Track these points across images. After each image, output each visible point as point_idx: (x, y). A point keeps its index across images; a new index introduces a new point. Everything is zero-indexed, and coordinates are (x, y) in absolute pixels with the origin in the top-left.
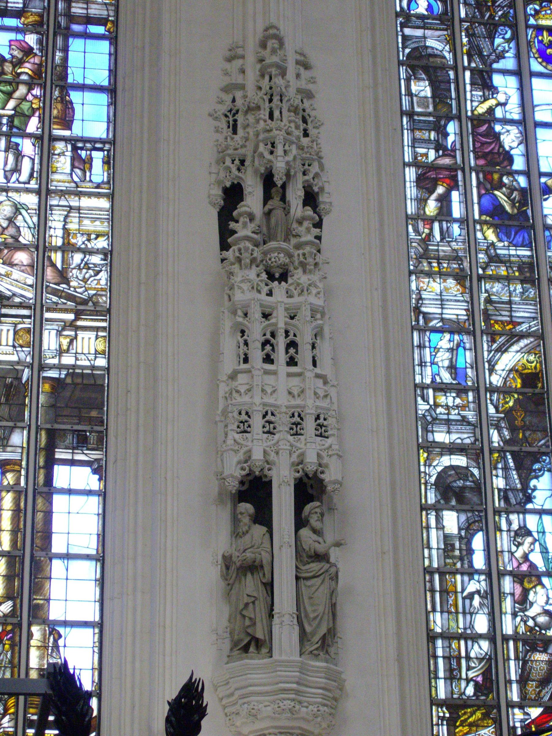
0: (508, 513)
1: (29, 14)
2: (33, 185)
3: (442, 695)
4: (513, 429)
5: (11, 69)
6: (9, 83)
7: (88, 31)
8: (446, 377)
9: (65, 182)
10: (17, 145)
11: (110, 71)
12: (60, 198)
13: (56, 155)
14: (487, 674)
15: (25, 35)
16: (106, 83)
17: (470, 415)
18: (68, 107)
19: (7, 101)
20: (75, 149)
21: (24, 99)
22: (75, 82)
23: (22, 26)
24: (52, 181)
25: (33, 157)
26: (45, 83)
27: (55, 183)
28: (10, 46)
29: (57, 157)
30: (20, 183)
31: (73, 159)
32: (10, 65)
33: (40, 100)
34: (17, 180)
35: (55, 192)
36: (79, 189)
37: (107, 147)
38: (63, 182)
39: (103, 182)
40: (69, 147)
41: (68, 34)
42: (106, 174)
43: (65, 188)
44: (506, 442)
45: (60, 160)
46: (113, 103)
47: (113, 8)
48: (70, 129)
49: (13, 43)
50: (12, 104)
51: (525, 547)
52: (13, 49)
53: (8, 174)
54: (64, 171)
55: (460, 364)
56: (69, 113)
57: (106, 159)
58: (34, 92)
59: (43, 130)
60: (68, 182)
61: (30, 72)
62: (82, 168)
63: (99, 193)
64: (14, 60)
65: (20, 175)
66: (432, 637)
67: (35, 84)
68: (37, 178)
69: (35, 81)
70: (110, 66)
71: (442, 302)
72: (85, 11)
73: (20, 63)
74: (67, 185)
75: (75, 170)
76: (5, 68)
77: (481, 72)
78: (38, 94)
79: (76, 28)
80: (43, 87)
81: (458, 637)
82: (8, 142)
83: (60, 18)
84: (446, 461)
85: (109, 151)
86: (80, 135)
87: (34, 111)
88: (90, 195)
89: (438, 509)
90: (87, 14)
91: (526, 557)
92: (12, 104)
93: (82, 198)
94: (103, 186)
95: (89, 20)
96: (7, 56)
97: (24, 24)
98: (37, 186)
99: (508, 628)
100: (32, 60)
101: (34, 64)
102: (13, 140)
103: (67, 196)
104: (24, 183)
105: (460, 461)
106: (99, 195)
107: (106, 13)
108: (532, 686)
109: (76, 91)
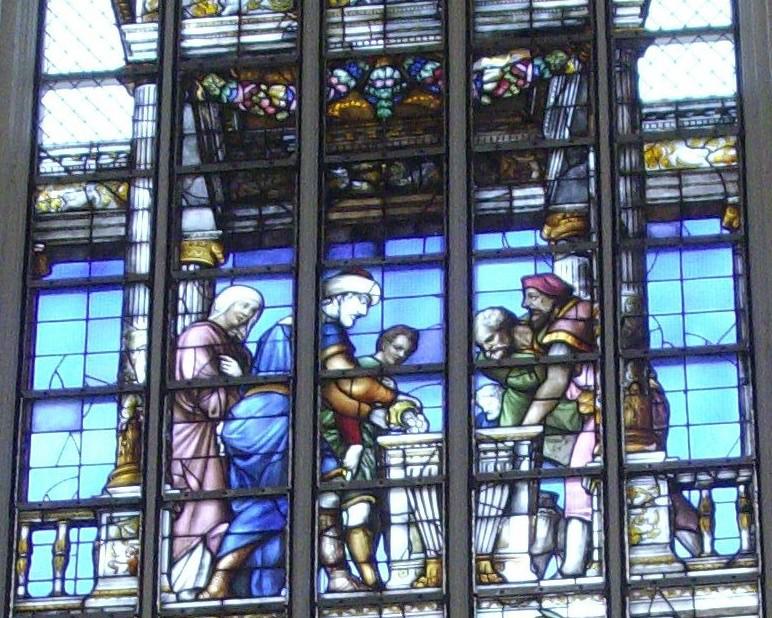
1: (559, 216)
2: (593, 578)
5: (529, 337)
6: (527, 368)
7: (685, 234)
9: (661, 562)
10: (554, 497)
11: (738, 311)
12: (652, 598)
13: (636, 507)
15: (554, 261)
16: (731, 339)
18: (655, 403)
19: (527, 408)
20: (676, 489)
21: (560, 398)
22: (666, 346)
23: (545, 243)
24: (632, 564)
25: (588, 518)
26: (603, 357)
27: (639, 568)
28: (524, 290)
29: (639, 511)
30: (565, 576)
31: (673, 512)
32: (527, 329)
33: (595, 395)
34: (560, 571)
35: (640, 586)
36: (692, 574)
37: (744, 475)
38: (654, 563)
39: (740, 553)
40: (664, 488)
41: (644, 246)
42: (745, 534)
43: (660, 576)
45: (645, 516)
46: (749, 380)
47: (735, 177)
48: (662, 447)
49: (529, 283)
50: (535, 412)
52: (531, 296)
53: (540, 561)
54: (657, 540)
56: (658, 415)
57: (743, 502)
58: (581, 380)
59: (605, 459)
60: (667, 563)
61: (569, 339)
62: (693, 526)
63: (734, 576)
64: (535, 318)
65: (564, 560)
67: (583, 363)
68: (600, 561)
69: (582, 357)
70: (736, 302)
72: (675, 193)
73: (547, 322)
74: (664, 567)
75: (679, 534)
76: (517, 337)
78: (591, 382)
79: (659, 230)
80: (598, 366)
82: (535, 494)
83: (623, 216)
85: (747, 483)
86: (685, 457)
87: (583, 419)
88: (713, 583)
90: (681, 197)
92: (535, 412)
93: (698, 593)
94: (742, 561)
95: (686, 210)
96: (520, 312)
97: (549, 240)
98: (601, 580)
100: (572, 314)
101: (577, 320)
102: (544, 487)
103: (665, 593)
104: (575, 576)
106: (732, 582)
107: (720, 189)
109: (666, 365)
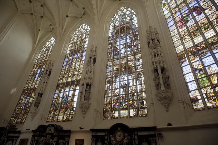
0: (114, 83)
3: (105, 103)
4: (115, 74)
8: (109, 71)
14: (110, 100)
17: (111, 74)
44: (114, 76)
51: (115, 86)
55: (111, 69)
66: (105, 97)
71: (110, 64)
77: (115, 42)
81: (107, 97)
84: (108, 79)
89: (107, 84)
91: (115, 87)
99: (113, 95)
105: (110, 79)
108: (114, 101)
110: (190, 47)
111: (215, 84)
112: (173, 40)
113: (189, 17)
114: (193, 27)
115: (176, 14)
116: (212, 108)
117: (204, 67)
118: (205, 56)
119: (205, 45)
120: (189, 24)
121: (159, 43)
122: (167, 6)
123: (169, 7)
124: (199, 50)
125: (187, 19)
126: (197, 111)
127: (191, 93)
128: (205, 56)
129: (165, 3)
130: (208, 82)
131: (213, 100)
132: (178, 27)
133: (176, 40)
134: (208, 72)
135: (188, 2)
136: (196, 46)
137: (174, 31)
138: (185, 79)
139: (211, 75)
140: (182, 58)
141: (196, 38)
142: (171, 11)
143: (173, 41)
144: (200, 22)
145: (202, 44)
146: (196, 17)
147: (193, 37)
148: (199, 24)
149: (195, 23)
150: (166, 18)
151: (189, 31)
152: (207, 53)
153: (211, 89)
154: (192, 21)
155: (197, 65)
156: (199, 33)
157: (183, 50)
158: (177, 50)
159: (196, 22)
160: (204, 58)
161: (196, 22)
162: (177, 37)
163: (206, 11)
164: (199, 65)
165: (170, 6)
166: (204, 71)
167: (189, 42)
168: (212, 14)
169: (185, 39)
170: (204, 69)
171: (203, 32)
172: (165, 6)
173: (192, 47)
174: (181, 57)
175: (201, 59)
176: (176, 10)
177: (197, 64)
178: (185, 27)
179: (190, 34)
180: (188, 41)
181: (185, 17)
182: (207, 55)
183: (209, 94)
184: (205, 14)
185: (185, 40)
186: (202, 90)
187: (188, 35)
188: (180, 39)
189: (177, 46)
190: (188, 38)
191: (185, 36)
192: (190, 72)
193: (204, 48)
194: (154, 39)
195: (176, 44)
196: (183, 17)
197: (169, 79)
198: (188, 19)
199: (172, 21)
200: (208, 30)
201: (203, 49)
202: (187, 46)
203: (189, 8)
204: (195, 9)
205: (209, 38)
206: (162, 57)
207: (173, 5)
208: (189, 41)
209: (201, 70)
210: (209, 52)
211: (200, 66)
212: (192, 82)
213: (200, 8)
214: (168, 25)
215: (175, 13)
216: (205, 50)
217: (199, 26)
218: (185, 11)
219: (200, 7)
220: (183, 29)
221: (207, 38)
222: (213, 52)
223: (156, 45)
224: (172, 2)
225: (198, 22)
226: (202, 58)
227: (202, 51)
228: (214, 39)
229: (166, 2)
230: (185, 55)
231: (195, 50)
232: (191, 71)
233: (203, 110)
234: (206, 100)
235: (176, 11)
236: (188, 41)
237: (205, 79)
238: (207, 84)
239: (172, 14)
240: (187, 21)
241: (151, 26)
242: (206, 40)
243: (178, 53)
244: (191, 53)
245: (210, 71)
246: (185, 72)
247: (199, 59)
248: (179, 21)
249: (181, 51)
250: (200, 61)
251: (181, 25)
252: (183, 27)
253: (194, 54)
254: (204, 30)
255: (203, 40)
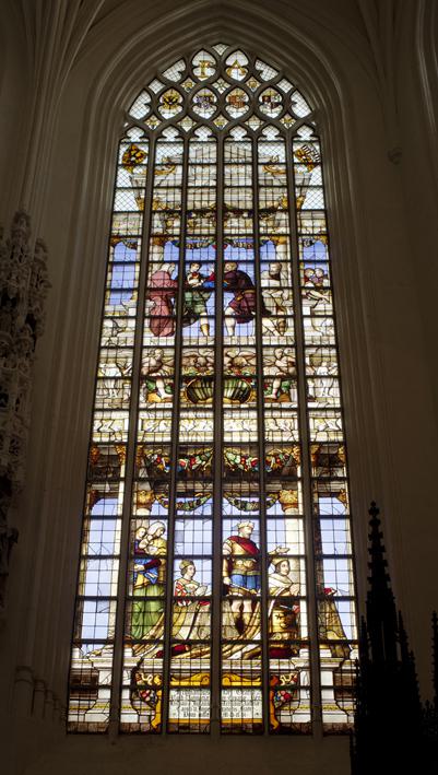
110: (154, 443)
111: (178, 641)
112: (102, 366)
113: (205, 301)
114: (201, 360)
115: (162, 244)
116: (134, 733)
117: (171, 556)
118: (192, 513)
119: (209, 464)
120: (191, 333)
121: (32, 341)
122: (139, 171)
123: (150, 187)
124: (183, 475)
125: (194, 303)
126: (76, 732)
127: (81, 653)
128: (190, 510)
129: (138, 150)
130: (159, 626)
131: (148, 703)
132: (144, 317)
133: (113, 371)
134: (175, 585)
135: (227, 231)
136: (177, 448)
137: (121, 323)
138: (81, 580)
139: (181, 599)
140: (107, 473)
141: (191, 415)
142: (148, 213)
143: (98, 368)
144: (231, 354)
145: (200, 455)
146: (229, 322)
147: (184, 401)
148: (226, 360)
149: (214, 347)
150: (115, 232)
151: (181, 366)
152: (203, 500)
153: (159, 655)
154: (208, 326)
155: (150, 538)
156: (210, 400)
157: (125, 438)
158: (97, 424)
159: (219, 346)
160: (184, 518)
161: (219, 346)
162: (121, 364)
163: (266, 322)
164: (156, 538)
165: (156, 184)
166: (162, 573)
167: (160, 415)
168: (278, 352)
169: (150, 391)
170: (166, 565)
171: (225, 406)
172: (134, 164)
173: (162, 445)
174: (98, 468)
175: (172, 518)
176: (170, 223)
177: (151, 531)
178: (173, 338)
179: (177, 381)
180: (156, 410)
181: (190, 289)
182: (198, 512)
183: (146, 673)
184: (259, 334)
185: (147, 394)
186: (128, 653)
187: (169, 381)
188: (131, 379)
189: (106, 406)
190: (164, 395)
191: (158, 377)
192: (112, 557)
193: (200, 475)
194: (15, 301)
195: (105, 392)
196: (181, 285)
197: (10, 546)
198: (199, 308)
199: (130, 268)
200: (243, 406)
201: (197, 475)
202: (146, 427)
203: (219, 262)
204: (239, 283)
205: (232, 444)
206: (22, 419)
207: (168, 187)
208: (164, 410)
209: (154, 563)
210: (211, 500)
211: (159, 543)
212: (103, 605)
213: (255, 294)
214: (109, 274)
215: (163, 239)
216: (199, 486)
217: (223, 371)
218: (200, 263)
219: (255, 289)
220: (163, 341)
221: (227, 439)
222: (221, 509)
223: (14, 340)
224: (171, 177)
225: (225, 351)
226: (180, 513)
227: (190, 486)
228: (246, 457)
229: (145, 149)
230: (123, 468)
231: (167, 465)
232: (117, 552)
233: (101, 733)
234: (126, 694)
235: (170, 231)
236: (156, 410)
237: (153, 606)
238: (152, 632)
239: (147, 233)
240: (191, 317)
241: (28, 218)
242: (219, 444)
243: (96, 439)
244: (149, 469)
245: (182, 582)
246: (92, 548)
247: (165, 512)
248: (162, 289)
249: (113, 438)
250: (165, 522)
251: (160, 317)
252: (167, 331)
253: (157, 481)
254: (231, 398)
255: (210, 438)
